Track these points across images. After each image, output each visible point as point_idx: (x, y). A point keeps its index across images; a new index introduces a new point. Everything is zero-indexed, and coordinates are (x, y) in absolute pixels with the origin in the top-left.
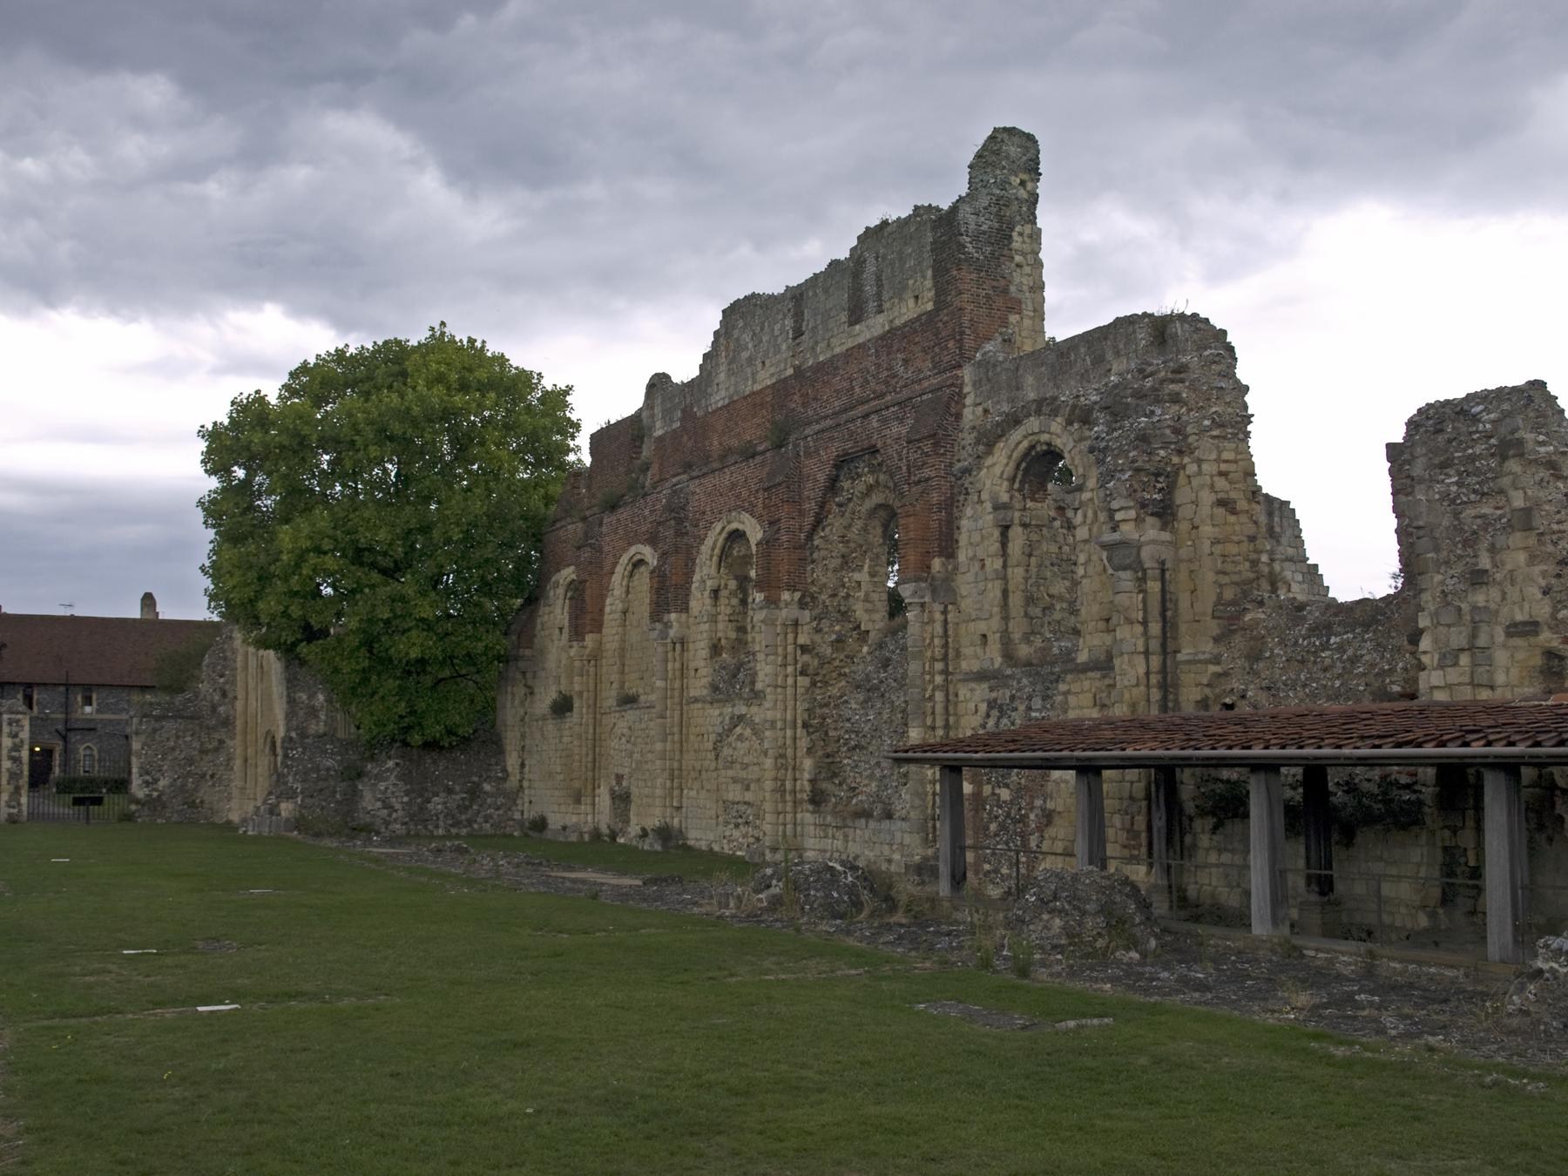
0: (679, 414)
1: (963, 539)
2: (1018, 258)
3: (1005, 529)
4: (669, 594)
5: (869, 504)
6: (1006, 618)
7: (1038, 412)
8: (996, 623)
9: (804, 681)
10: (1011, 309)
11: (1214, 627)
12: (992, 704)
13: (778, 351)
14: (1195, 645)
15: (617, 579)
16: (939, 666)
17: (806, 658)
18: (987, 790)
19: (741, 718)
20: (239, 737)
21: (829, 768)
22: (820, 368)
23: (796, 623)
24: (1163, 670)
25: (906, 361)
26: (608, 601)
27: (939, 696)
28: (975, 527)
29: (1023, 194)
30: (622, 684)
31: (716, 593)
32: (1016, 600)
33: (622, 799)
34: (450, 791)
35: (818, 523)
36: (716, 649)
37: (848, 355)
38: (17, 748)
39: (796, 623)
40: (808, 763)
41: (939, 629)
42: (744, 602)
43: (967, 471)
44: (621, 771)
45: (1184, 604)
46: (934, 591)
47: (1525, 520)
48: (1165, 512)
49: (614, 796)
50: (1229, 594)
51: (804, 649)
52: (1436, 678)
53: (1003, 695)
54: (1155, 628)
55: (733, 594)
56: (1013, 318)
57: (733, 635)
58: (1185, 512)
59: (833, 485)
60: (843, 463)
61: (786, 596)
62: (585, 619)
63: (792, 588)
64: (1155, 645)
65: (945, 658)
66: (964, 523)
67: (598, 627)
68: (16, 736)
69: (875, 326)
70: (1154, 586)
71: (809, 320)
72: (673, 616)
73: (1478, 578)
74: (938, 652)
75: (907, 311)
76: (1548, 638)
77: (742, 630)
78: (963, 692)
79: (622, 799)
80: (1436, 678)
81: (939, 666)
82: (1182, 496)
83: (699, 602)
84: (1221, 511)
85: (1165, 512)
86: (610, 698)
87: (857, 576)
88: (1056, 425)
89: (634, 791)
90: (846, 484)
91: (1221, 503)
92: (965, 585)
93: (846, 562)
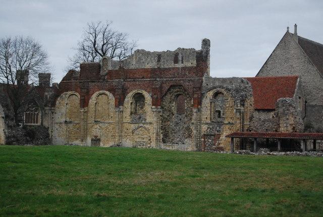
0: (118, 67)
1: (203, 103)
5: (176, 94)
7: (220, 88)
8: (209, 116)
12: (208, 128)
14: (247, 123)
15: (94, 96)
18: (206, 140)
19: (141, 127)
21: (166, 135)
22: (166, 69)
25: (189, 73)
31: (131, 103)
33: (96, 140)
36: (131, 113)
37: (173, 68)
40: (162, 135)
42: (136, 105)
44: (96, 135)
45: (245, 117)
46: (199, 110)
47: (292, 113)
48: (243, 105)
51: (161, 116)
52: (282, 129)
53: (211, 127)
54: (242, 120)
58: (246, 105)
59: (169, 90)
61: (159, 107)
66: (203, 101)
69: (180, 65)
71: (162, 60)
72: (121, 107)
73: (288, 119)
75: (189, 65)
76: (294, 126)
77: (136, 110)
78: (202, 125)
79: (96, 140)
80: (282, 129)
82: (246, 103)
85: (243, 105)
88: (223, 90)
89: (102, 139)
92: (203, 110)
93: (170, 102)
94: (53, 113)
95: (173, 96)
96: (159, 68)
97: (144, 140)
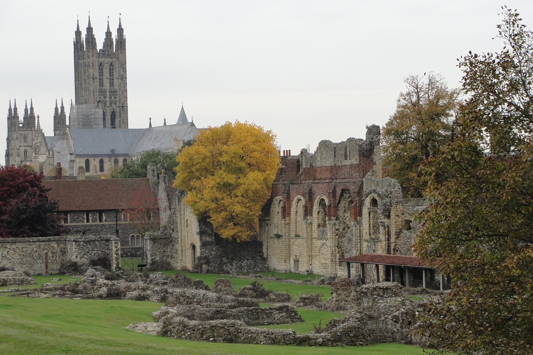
2: (375, 153)
3: (370, 213)
4: (308, 211)
6: (370, 229)
9: (337, 237)
10: (374, 165)
11: (395, 237)
13: (331, 159)
15: (294, 203)
16: (359, 238)
17: (337, 232)
20: (179, 244)
23: (335, 224)
24: (388, 243)
26: (292, 208)
27: (359, 244)
28: (365, 211)
29: (376, 140)
30: (296, 232)
31: (319, 212)
32: (371, 226)
33: (297, 261)
34: (248, 260)
35: (339, 202)
36: (319, 226)
38: (117, 251)
39: (335, 224)
40: (338, 255)
41: (359, 231)
43: (364, 200)
46: (358, 223)
49: (295, 261)
50: (398, 231)
51: (337, 230)
53: (369, 244)
54: (387, 236)
55: (323, 213)
56: (374, 166)
57: (323, 223)
60: (343, 190)
61: (333, 218)
62: (286, 212)
63: (334, 216)
64: (387, 239)
65: (360, 237)
67: (289, 215)
68: (117, 247)
70: (387, 229)
74: (359, 235)
78: (363, 243)
79: (297, 261)
81: (359, 238)
83: (315, 214)
84: (396, 217)
85: (389, 217)
86: (293, 234)
87: (347, 215)
89: (300, 260)
90: (345, 195)
91: (397, 216)
94: (267, 225)
95: (347, 204)
96: (335, 166)
97: (327, 262)
